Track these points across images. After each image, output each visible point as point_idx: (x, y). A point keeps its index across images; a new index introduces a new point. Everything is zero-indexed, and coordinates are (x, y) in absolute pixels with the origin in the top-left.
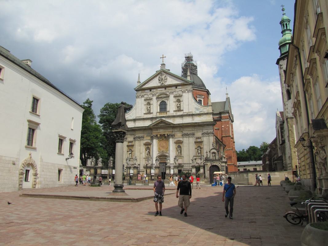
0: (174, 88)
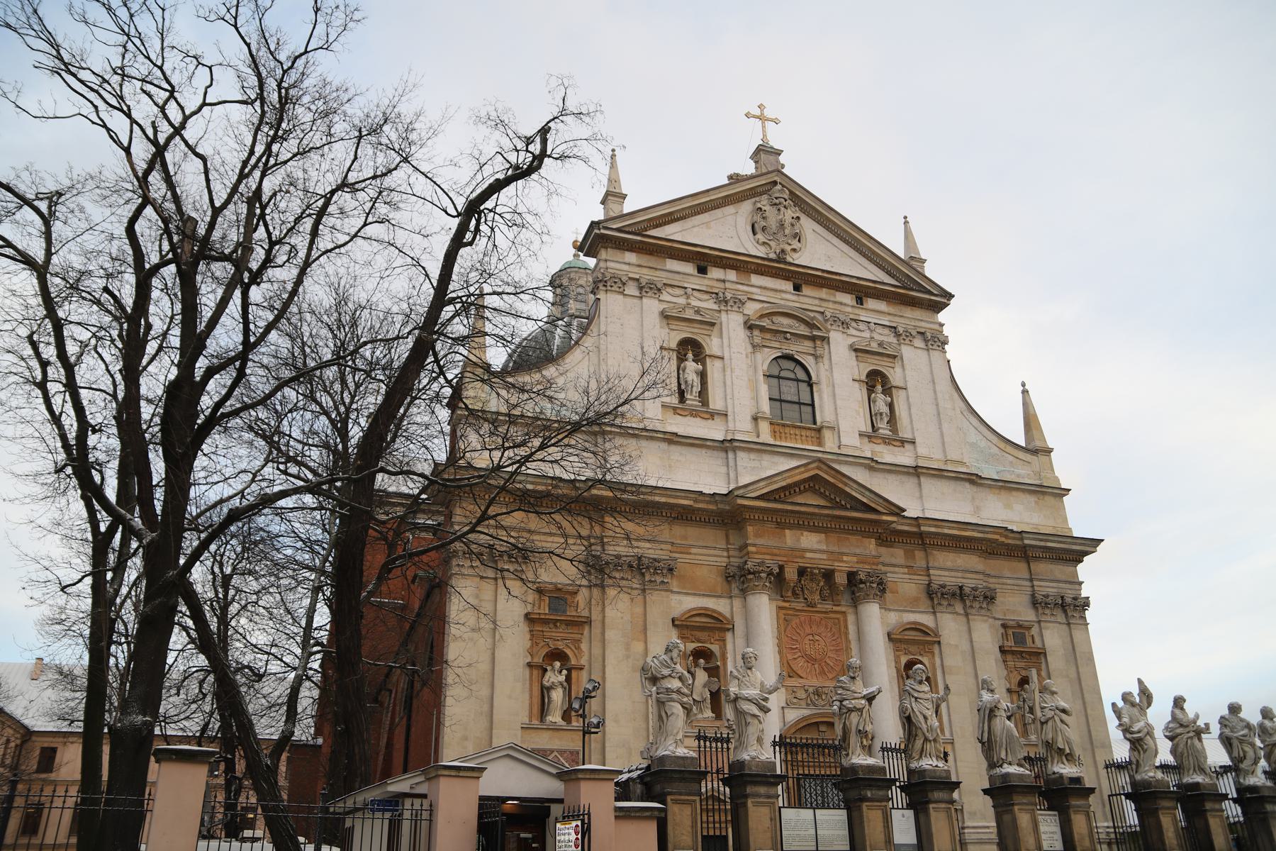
0: (848, 299)
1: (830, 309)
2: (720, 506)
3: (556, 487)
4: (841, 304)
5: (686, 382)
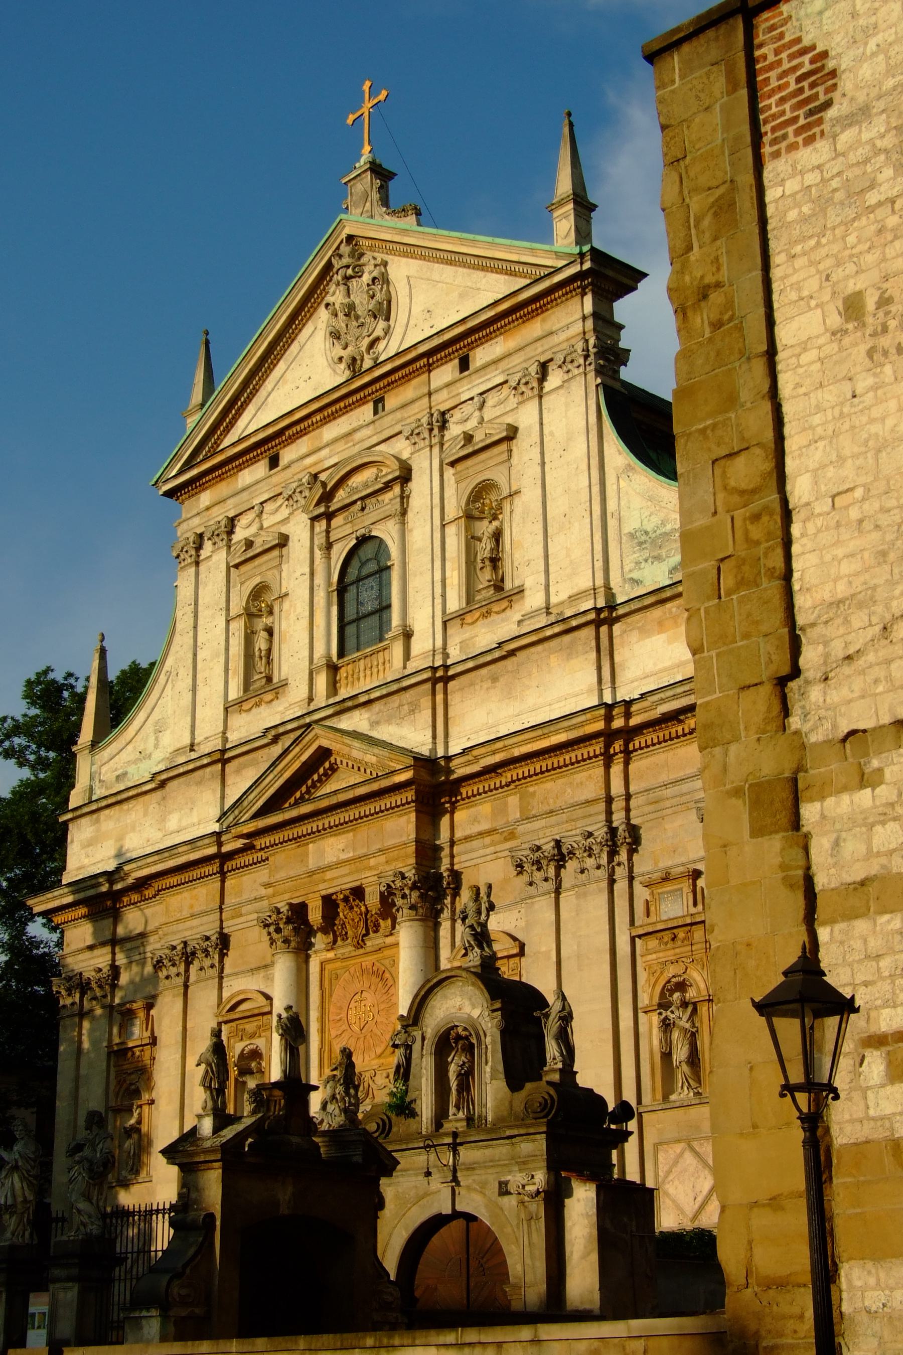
0: (445, 373)
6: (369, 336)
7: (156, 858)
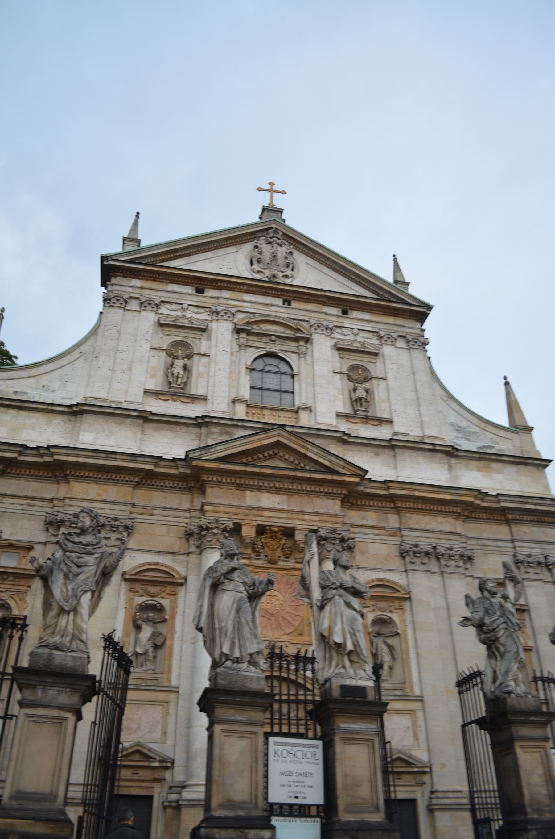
1: (314, 318)
2: (182, 470)
3: (20, 454)
4: (326, 314)
5: (173, 374)
6: (282, 272)
7: (90, 454)
